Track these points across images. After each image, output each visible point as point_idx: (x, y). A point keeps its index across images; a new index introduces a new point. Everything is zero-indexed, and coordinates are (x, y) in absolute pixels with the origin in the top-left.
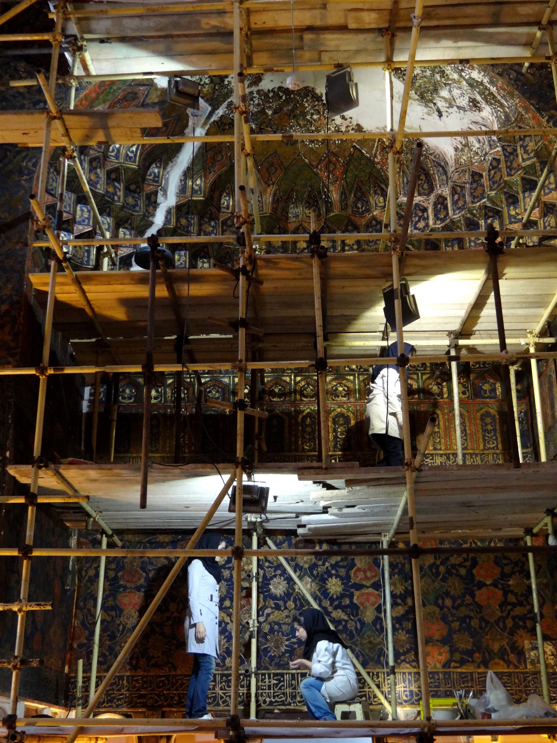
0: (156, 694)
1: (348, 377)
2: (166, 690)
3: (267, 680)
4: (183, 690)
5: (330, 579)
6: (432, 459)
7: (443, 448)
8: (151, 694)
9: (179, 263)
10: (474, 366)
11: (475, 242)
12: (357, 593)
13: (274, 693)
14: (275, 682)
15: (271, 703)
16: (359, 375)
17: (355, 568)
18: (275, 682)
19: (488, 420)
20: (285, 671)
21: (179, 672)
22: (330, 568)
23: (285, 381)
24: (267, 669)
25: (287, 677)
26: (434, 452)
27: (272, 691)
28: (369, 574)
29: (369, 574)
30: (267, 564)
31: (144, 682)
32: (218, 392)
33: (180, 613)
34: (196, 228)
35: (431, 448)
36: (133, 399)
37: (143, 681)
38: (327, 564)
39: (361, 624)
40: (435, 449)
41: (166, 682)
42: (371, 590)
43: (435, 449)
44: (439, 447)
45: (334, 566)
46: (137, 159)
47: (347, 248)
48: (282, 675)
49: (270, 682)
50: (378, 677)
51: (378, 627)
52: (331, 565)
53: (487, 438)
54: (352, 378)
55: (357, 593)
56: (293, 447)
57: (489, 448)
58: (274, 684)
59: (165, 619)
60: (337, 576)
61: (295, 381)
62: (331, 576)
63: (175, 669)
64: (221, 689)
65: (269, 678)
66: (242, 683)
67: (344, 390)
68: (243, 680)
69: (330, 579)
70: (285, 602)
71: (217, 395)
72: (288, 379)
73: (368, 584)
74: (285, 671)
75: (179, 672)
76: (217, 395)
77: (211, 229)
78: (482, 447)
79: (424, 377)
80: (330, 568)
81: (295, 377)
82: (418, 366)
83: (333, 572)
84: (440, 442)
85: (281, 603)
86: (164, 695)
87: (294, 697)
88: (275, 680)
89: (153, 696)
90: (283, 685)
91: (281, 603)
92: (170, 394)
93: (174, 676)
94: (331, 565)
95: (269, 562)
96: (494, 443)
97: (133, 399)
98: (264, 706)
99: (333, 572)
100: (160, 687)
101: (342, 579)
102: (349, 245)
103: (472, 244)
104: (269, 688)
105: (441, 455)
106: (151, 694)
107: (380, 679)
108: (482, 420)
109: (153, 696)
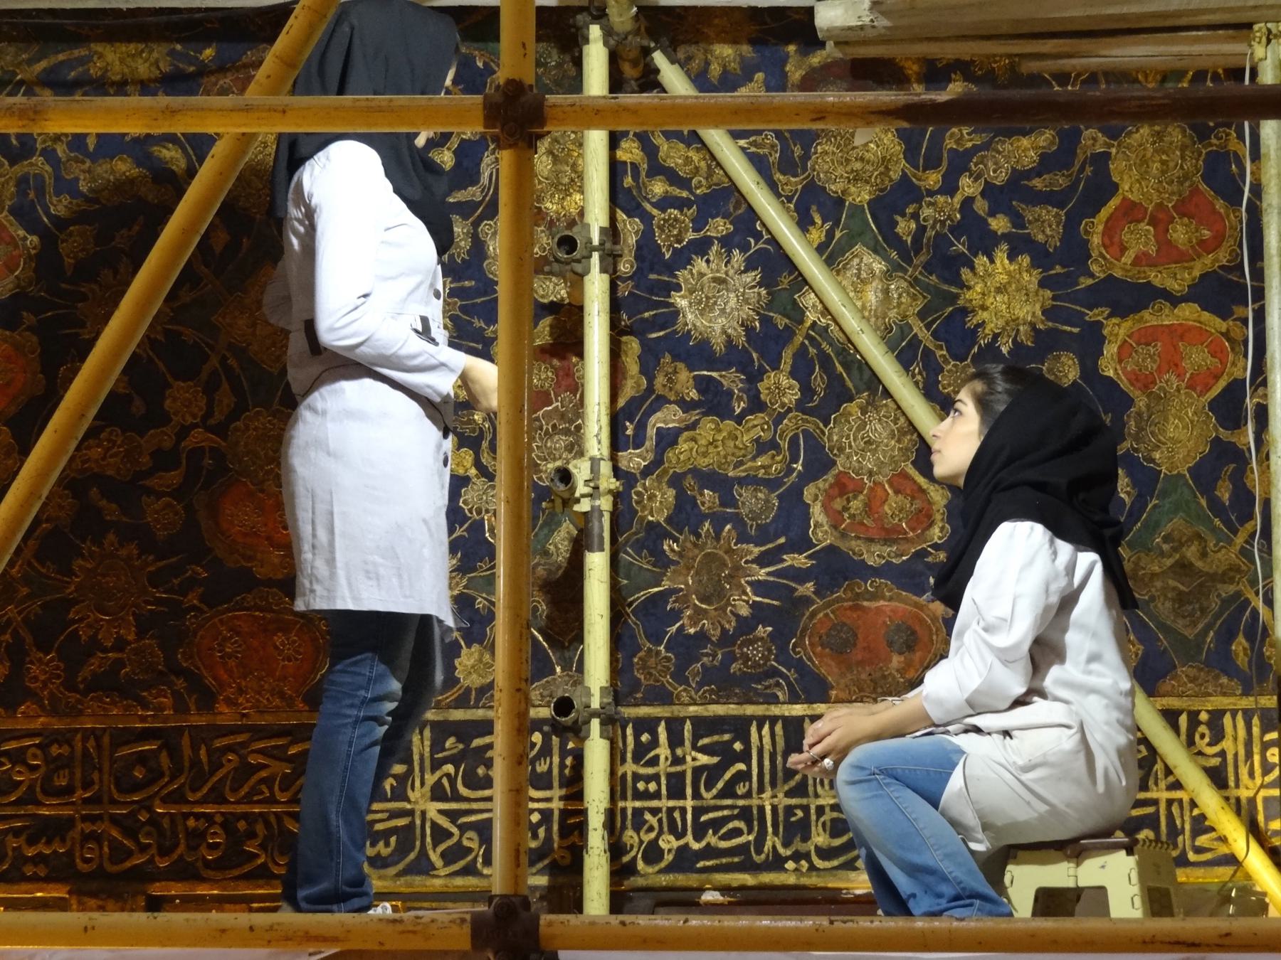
0: (115, 820)
2: (164, 801)
3: (663, 751)
4: (247, 799)
5: (981, 261)
8: (93, 819)
12: (1117, 331)
13: (698, 812)
14: (704, 759)
15: (684, 860)
17: (1114, 203)
18: (704, 759)
20: (750, 710)
21: (225, 715)
22: (981, 206)
24: (664, 697)
25: (761, 738)
27: (689, 803)
28: (1180, 234)
29: (1180, 234)
30: (658, 188)
31: (56, 764)
33: (221, 430)
37: (48, 760)
38: (968, 187)
39: (1135, 483)
41: (165, 760)
42: (1189, 313)
45: (998, 197)
48: (740, 727)
49: (677, 761)
50: (1218, 736)
51: (1224, 493)
52: (989, 191)
55: (1117, 331)
58: (697, 771)
59: (145, 460)
60: (1019, 245)
62: (985, 243)
63: (207, 700)
64: (437, 794)
65: (675, 740)
66: (542, 767)
68: (546, 751)
69: (981, 261)
70: (753, 377)
73: (1176, 280)
74: (750, 710)
75: (225, 715)
80: (981, 206)
83: (999, 224)
85: (731, 379)
86: (154, 821)
87: (796, 829)
88: (705, 750)
89: (99, 828)
90: (744, 776)
91: (731, 379)
93: (200, 736)
94: (989, 191)
95: (672, 177)
98: (648, 874)
99: (999, 224)
100: (136, 787)
101: (1041, 257)
104: (676, 791)
106: (93, 819)
107: (1227, 744)
109: (99, 828)
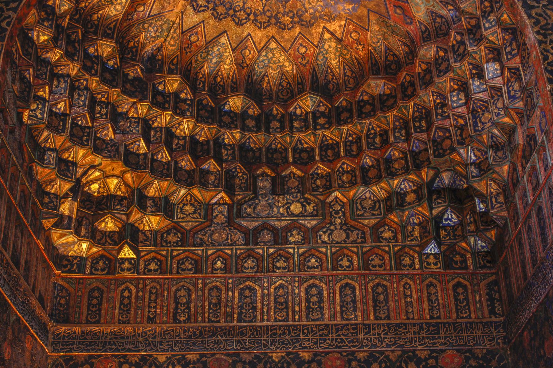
1: (321, 249)
6: (406, 329)
7: (416, 318)
9: (155, 138)
10: (445, 238)
11: (442, 116)
16: (331, 247)
19: (460, 290)
23: (258, 253)
26: (407, 321)
32: (191, 263)
34: (172, 104)
35: (404, 318)
36: (106, 271)
40: (408, 318)
43: (408, 318)
44: (411, 316)
46: (115, 36)
47: (318, 127)
53: (459, 307)
54: (324, 250)
56: (265, 317)
57: (462, 318)
61: (267, 253)
67: (316, 261)
71: (190, 266)
72: (260, 251)
76: (190, 266)
77: (187, 107)
78: (454, 315)
79: (396, 249)
81: (268, 249)
82: (390, 238)
84: (412, 311)
92: (143, 266)
96: (466, 313)
97: (106, 271)
102: (320, 125)
103: (439, 117)
105: (414, 325)
108: (454, 290)
